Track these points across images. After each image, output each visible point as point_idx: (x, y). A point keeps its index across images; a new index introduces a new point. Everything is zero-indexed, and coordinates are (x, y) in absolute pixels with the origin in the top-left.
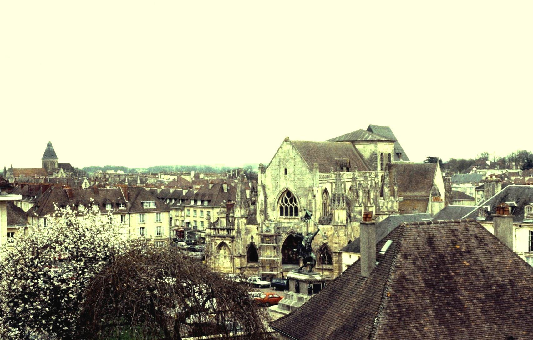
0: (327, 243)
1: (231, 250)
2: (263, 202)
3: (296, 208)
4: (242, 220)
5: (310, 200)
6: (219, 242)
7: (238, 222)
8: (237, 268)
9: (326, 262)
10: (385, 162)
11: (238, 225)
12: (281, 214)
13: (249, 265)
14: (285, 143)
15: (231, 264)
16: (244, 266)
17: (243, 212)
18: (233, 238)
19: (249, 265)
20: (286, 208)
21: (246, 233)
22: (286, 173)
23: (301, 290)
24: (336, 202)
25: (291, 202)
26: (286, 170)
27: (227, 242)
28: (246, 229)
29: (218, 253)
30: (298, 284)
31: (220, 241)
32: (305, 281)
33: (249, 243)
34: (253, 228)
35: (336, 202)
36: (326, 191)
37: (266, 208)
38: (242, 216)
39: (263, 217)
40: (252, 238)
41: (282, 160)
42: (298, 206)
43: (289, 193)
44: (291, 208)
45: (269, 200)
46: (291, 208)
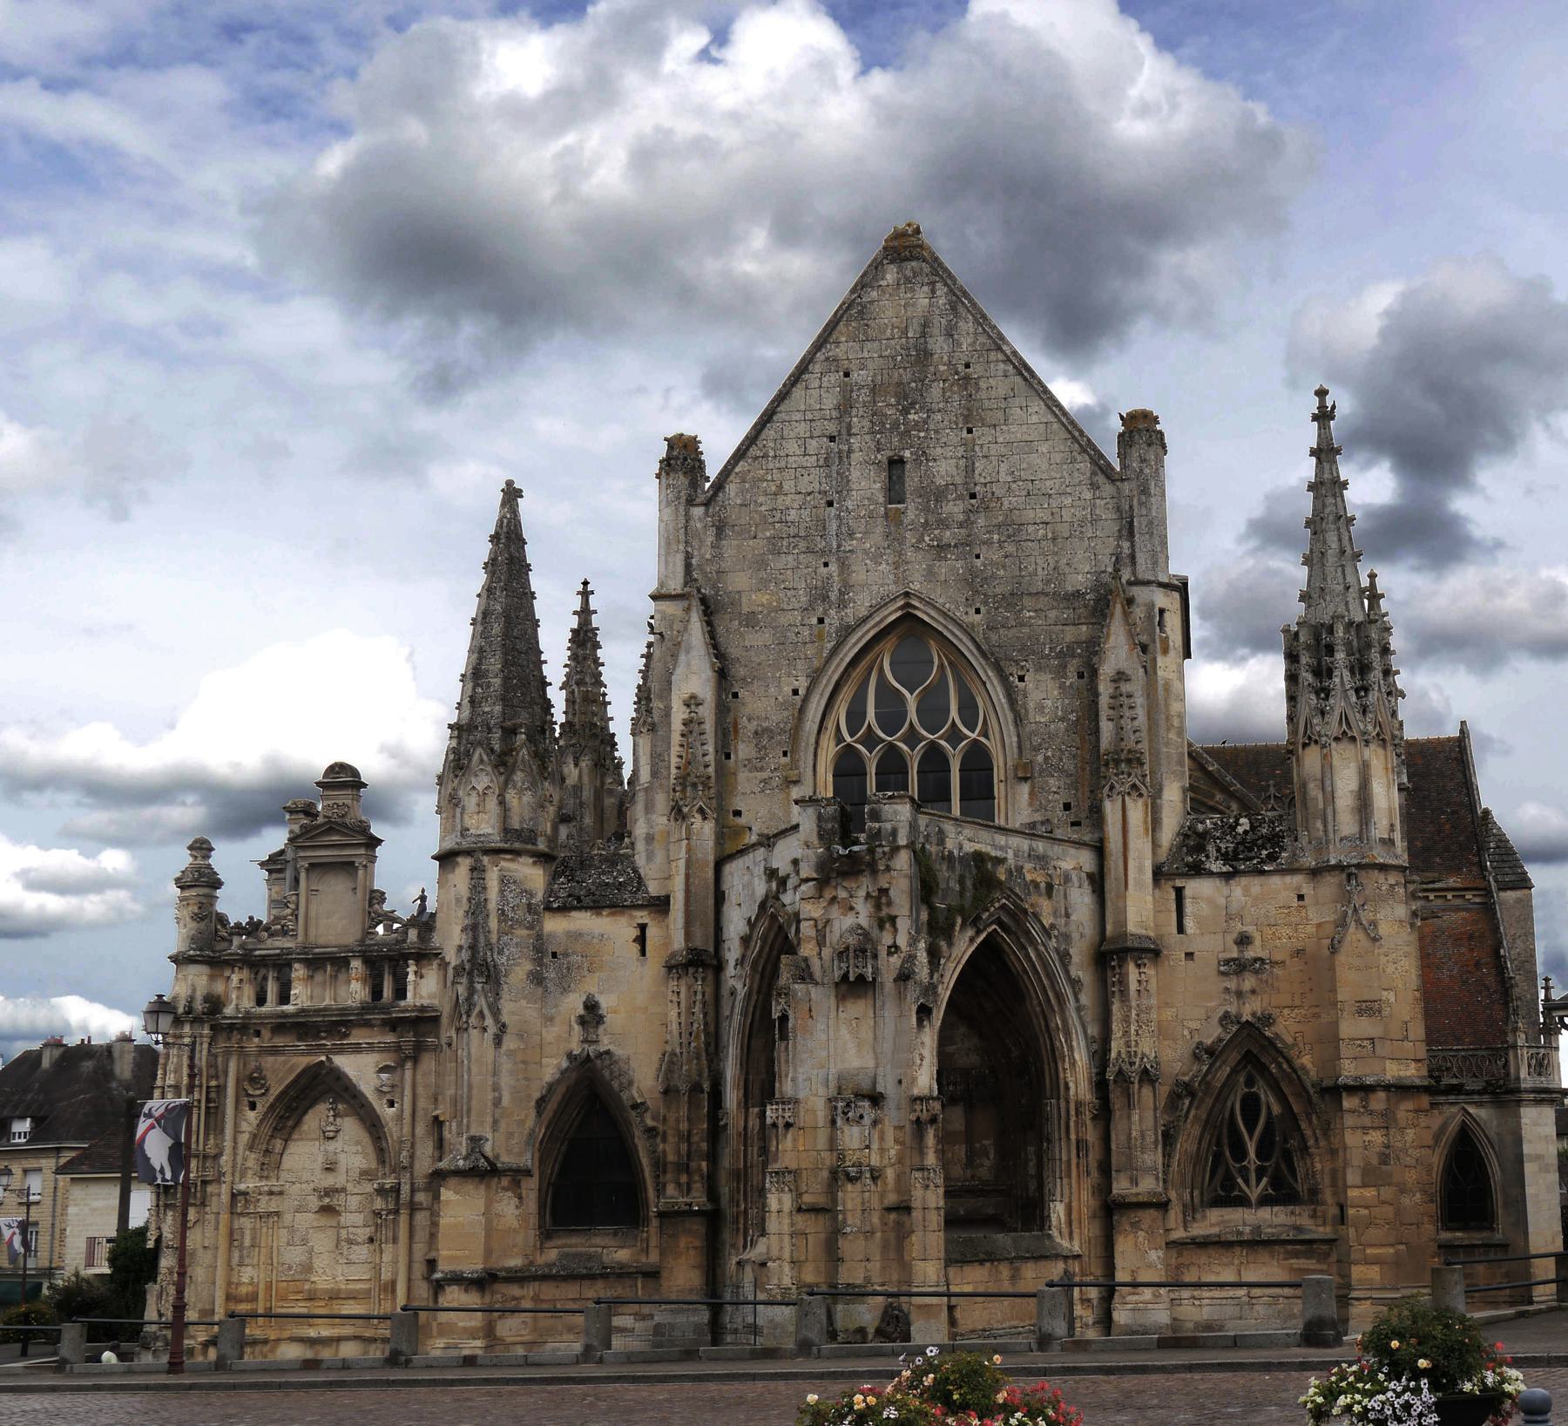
0: (1268, 1020)
2: (707, 712)
3: (978, 763)
4: (506, 864)
5: (1120, 677)
8: (457, 1279)
9: (1254, 1193)
13: (552, 1255)
14: (891, 275)
16: (515, 1262)
17: (521, 803)
18: (425, 1021)
21: (537, 979)
24: (1342, 678)
25: (933, 712)
26: (896, 463)
27: (361, 1068)
28: (542, 951)
29: (270, 1164)
35: (1342, 678)
37: (724, 776)
38: (506, 831)
40: (592, 1015)
41: (864, 396)
44: (933, 751)
45: (762, 704)
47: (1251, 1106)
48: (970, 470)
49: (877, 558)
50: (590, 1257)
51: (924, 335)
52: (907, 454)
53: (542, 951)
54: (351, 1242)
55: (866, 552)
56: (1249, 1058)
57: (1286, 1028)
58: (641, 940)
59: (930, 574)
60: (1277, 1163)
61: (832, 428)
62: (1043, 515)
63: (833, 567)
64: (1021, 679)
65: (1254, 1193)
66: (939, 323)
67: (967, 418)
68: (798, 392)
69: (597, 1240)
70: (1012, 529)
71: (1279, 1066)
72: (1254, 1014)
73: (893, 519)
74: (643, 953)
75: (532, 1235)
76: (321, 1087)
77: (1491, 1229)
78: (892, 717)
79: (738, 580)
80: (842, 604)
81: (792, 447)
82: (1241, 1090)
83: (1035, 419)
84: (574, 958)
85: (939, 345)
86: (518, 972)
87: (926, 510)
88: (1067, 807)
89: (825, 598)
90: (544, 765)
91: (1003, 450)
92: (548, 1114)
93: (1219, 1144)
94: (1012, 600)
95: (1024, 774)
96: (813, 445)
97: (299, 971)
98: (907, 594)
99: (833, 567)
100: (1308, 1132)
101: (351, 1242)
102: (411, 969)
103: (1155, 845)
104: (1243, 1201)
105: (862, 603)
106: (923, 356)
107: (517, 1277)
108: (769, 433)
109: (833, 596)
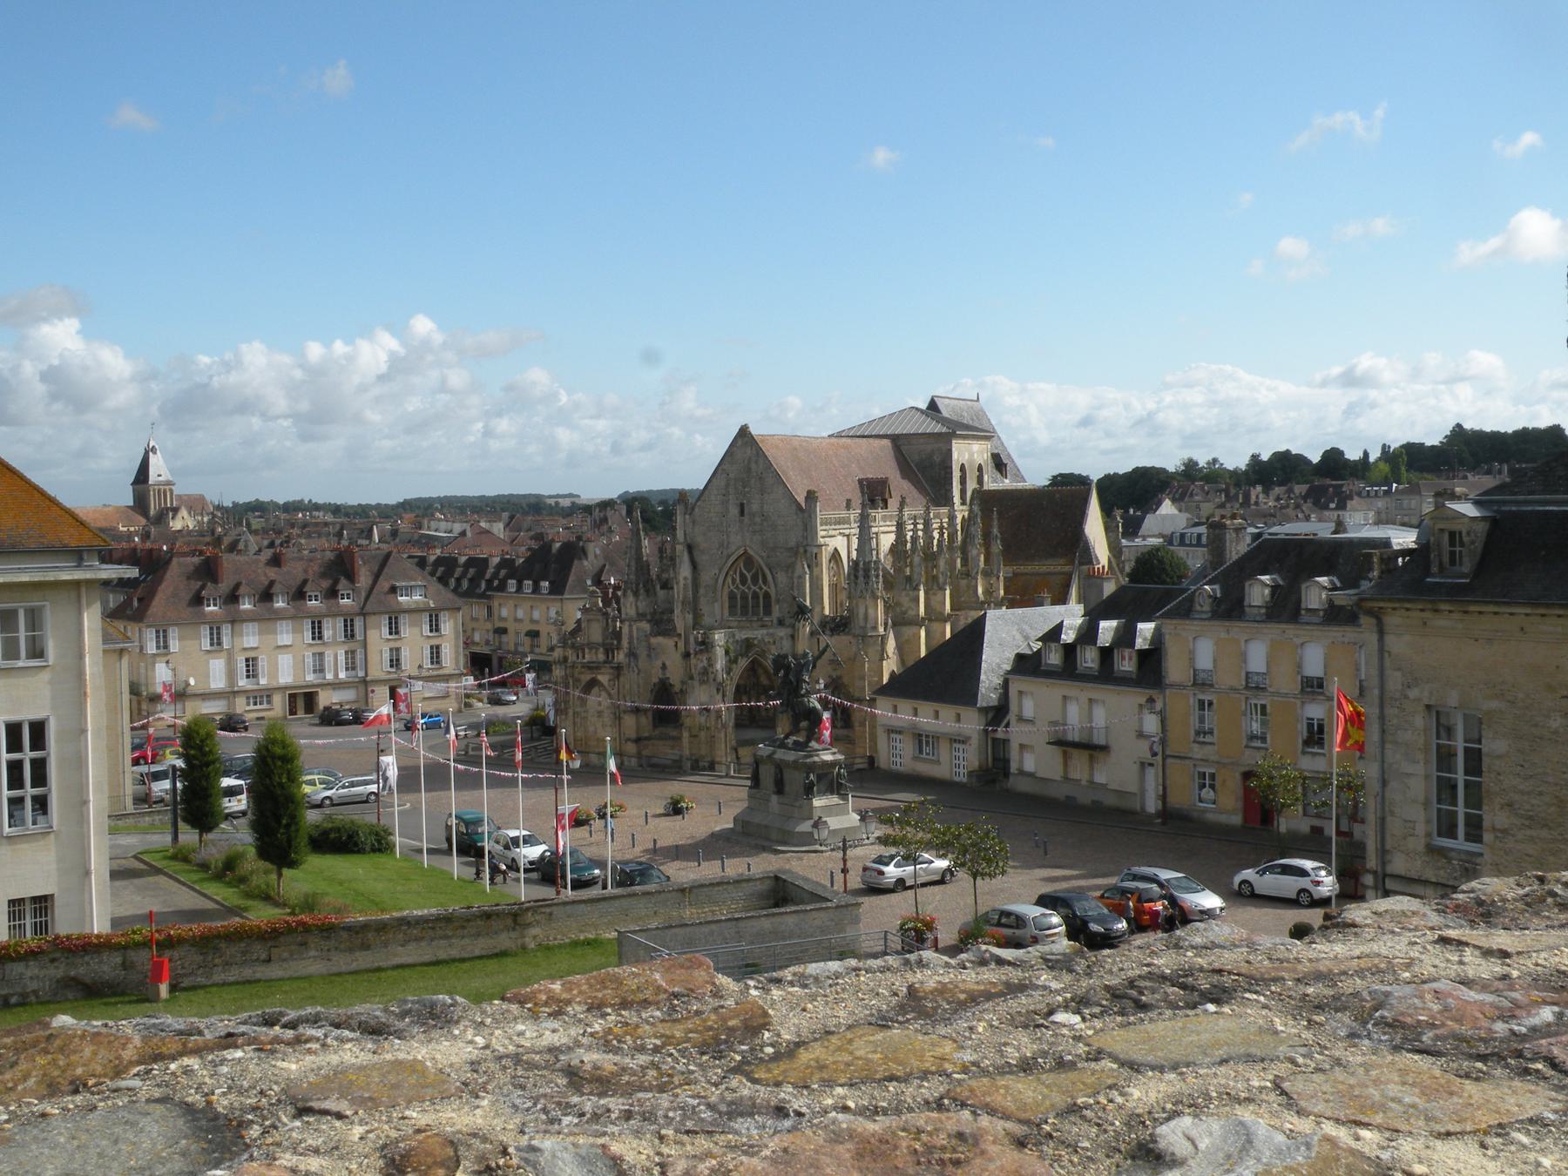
3: (767, 596)
6: (586, 677)
7: (631, 631)
8: (628, 740)
10: (971, 485)
11: (631, 637)
12: (732, 607)
18: (618, 669)
20: (744, 597)
21: (649, 656)
23: (787, 789)
24: (861, 579)
25: (755, 580)
26: (742, 505)
27: (603, 678)
30: (781, 772)
32: (795, 765)
33: (655, 680)
34: (667, 642)
35: (861, 579)
36: (835, 555)
39: (690, 617)
40: (664, 667)
42: (772, 592)
43: (748, 560)
44: (755, 593)
45: (706, 577)
46: (755, 596)
53: (650, 648)
73: (741, 522)
76: (593, 683)
78: (744, 581)
79: (699, 539)
85: (753, 466)
86: (642, 652)
90: (649, 591)
95: (778, 601)
105: (733, 548)
106: (749, 470)
107: (647, 739)
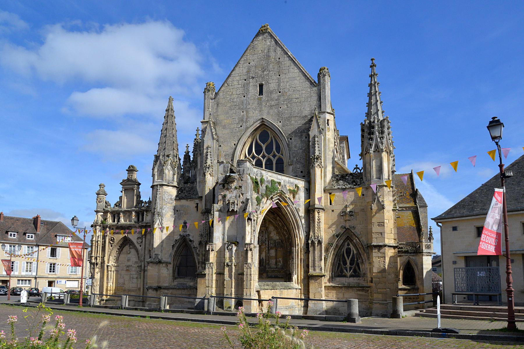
1: (141, 252)
13: (176, 283)
15: (140, 281)
16: (167, 285)
19: (176, 283)
22: (261, 93)
26: (261, 86)
27: (133, 237)
31: (121, 236)
47: (348, 251)
48: (279, 85)
49: (255, 110)
50: (184, 284)
51: (268, 52)
52: (263, 83)
54: (133, 278)
55: (253, 108)
56: (348, 238)
57: (357, 231)
58: (197, 207)
59: (268, 113)
60: (355, 267)
61: (245, 77)
62: (297, 96)
63: (245, 113)
64: (291, 139)
65: (348, 274)
66: (272, 48)
67: (279, 72)
68: (237, 69)
69: (186, 280)
70: (289, 100)
71: (356, 240)
72: (349, 226)
73: (260, 99)
74: (197, 210)
75: (171, 278)
77: (415, 285)
80: (246, 122)
81: (235, 83)
82: (346, 246)
83: (296, 71)
84: (182, 211)
85: (272, 54)
87: (268, 96)
88: (302, 172)
89: (242, 120)
91: (288, 80)
92: (175, 249)
93: (340, 261)
94: (289, 119)
96: (240, 82)
97: (122, 215)
98: (262, 118)
99: (245, 113)
100: (363, 258)
101: (133, 278)
102: (145, 214)
103: (325, 181)
104: (345, 276)
105: (251, 121)
108: (230, 79)
109: (245, 120)
